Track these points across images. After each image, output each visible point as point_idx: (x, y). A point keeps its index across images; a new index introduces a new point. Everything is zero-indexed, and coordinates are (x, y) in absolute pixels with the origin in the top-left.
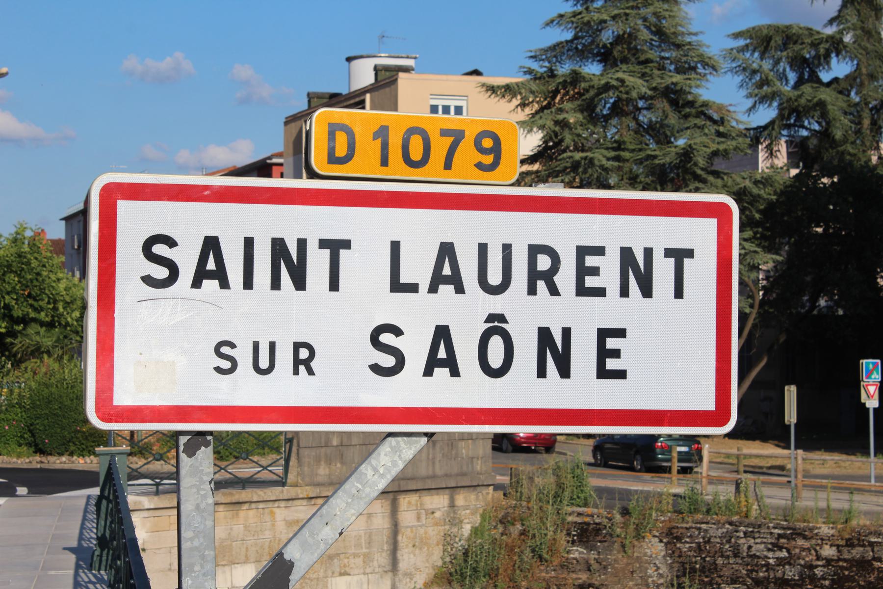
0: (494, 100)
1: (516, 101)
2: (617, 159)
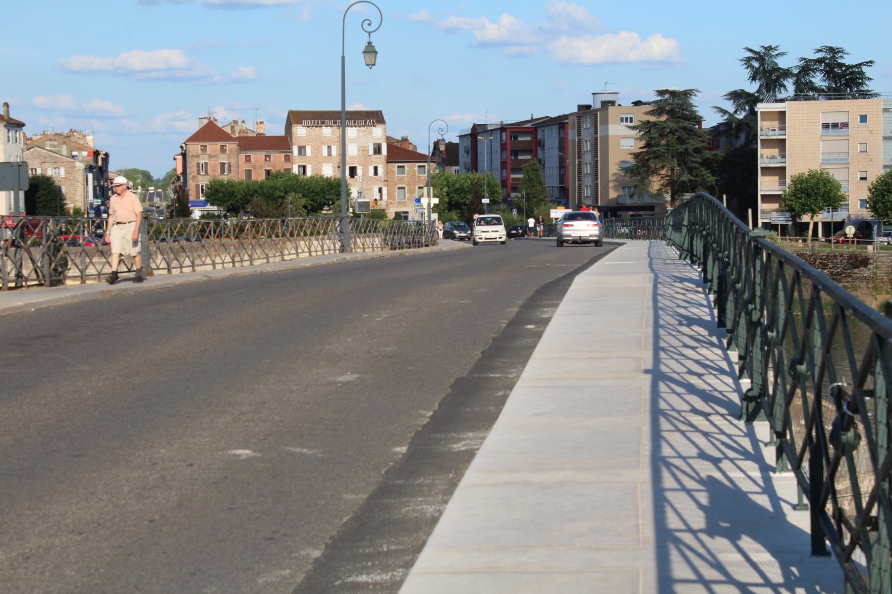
0: (630, 130)
1: (638, 131)
2: (667, 149)
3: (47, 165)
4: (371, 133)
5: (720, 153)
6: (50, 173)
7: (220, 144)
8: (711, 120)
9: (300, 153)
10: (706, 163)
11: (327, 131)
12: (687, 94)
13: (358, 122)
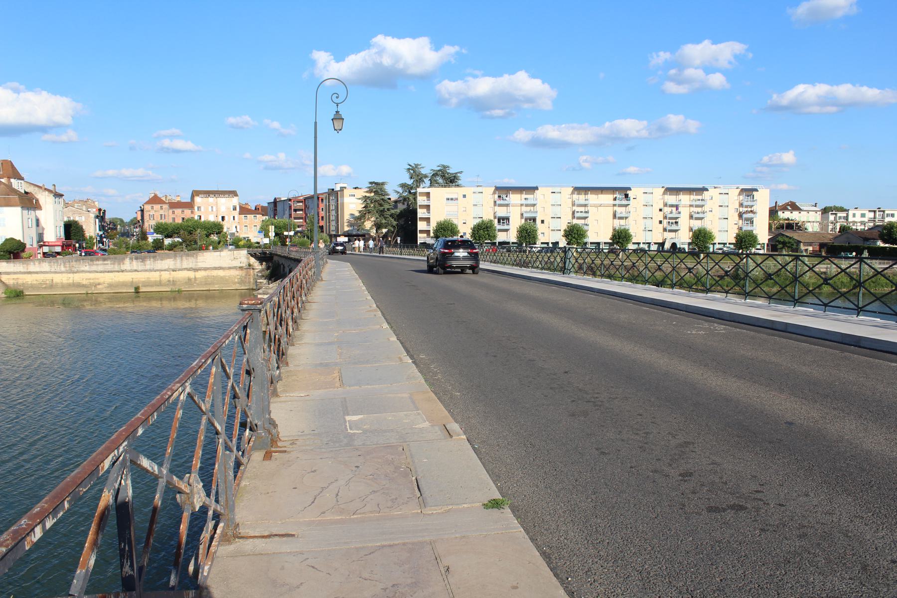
3: (76, 215)
4: (231, 201)
5: (398, 211)
6: (77, 219)
7: (160, 205)
8: (394, 197)
9: (198, 210)
10: (392, 215)
11: (211, 200)
12: (383, 184)
13: (227, 196)
